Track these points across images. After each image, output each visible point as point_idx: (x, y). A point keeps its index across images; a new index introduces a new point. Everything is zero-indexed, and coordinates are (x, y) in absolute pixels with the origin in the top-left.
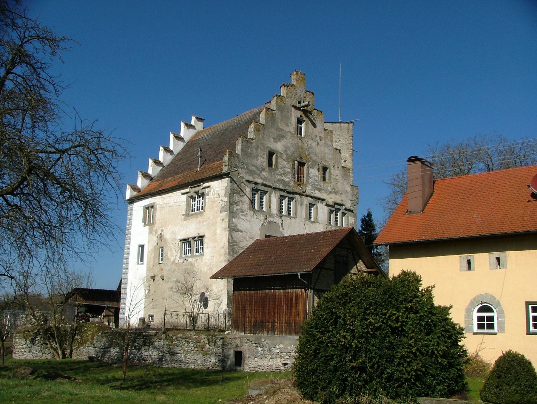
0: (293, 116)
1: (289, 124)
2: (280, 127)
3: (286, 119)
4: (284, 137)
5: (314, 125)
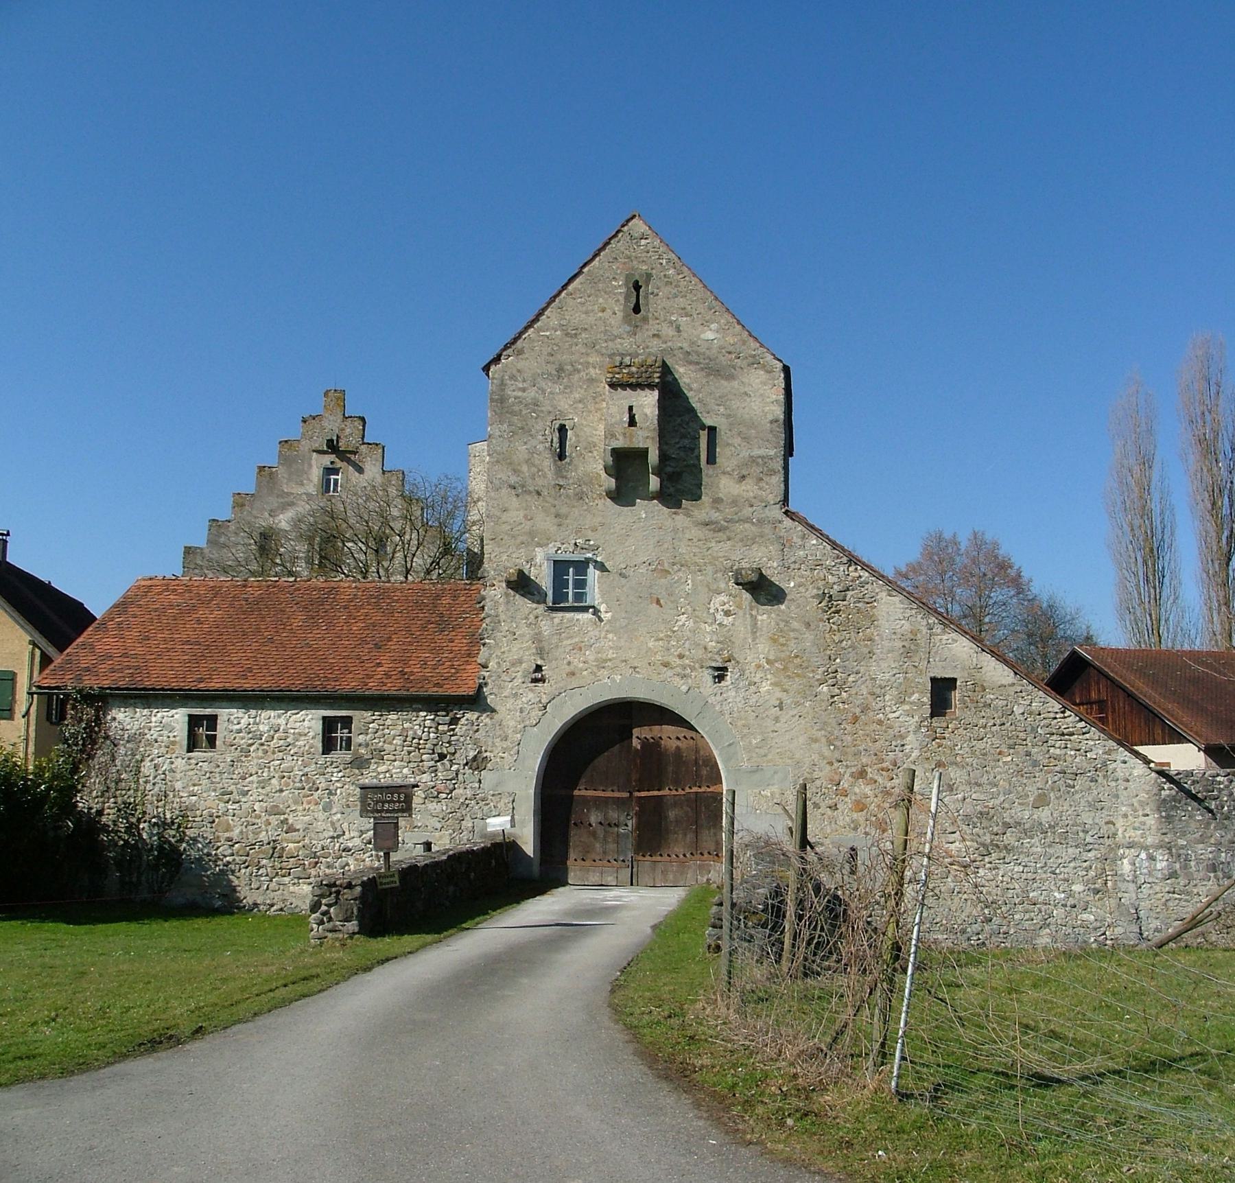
0: (315, 467)
1: (305, 482)
2: (286, 490)
3: (299, 476)
4: (292, 504)
5: (360, 470)
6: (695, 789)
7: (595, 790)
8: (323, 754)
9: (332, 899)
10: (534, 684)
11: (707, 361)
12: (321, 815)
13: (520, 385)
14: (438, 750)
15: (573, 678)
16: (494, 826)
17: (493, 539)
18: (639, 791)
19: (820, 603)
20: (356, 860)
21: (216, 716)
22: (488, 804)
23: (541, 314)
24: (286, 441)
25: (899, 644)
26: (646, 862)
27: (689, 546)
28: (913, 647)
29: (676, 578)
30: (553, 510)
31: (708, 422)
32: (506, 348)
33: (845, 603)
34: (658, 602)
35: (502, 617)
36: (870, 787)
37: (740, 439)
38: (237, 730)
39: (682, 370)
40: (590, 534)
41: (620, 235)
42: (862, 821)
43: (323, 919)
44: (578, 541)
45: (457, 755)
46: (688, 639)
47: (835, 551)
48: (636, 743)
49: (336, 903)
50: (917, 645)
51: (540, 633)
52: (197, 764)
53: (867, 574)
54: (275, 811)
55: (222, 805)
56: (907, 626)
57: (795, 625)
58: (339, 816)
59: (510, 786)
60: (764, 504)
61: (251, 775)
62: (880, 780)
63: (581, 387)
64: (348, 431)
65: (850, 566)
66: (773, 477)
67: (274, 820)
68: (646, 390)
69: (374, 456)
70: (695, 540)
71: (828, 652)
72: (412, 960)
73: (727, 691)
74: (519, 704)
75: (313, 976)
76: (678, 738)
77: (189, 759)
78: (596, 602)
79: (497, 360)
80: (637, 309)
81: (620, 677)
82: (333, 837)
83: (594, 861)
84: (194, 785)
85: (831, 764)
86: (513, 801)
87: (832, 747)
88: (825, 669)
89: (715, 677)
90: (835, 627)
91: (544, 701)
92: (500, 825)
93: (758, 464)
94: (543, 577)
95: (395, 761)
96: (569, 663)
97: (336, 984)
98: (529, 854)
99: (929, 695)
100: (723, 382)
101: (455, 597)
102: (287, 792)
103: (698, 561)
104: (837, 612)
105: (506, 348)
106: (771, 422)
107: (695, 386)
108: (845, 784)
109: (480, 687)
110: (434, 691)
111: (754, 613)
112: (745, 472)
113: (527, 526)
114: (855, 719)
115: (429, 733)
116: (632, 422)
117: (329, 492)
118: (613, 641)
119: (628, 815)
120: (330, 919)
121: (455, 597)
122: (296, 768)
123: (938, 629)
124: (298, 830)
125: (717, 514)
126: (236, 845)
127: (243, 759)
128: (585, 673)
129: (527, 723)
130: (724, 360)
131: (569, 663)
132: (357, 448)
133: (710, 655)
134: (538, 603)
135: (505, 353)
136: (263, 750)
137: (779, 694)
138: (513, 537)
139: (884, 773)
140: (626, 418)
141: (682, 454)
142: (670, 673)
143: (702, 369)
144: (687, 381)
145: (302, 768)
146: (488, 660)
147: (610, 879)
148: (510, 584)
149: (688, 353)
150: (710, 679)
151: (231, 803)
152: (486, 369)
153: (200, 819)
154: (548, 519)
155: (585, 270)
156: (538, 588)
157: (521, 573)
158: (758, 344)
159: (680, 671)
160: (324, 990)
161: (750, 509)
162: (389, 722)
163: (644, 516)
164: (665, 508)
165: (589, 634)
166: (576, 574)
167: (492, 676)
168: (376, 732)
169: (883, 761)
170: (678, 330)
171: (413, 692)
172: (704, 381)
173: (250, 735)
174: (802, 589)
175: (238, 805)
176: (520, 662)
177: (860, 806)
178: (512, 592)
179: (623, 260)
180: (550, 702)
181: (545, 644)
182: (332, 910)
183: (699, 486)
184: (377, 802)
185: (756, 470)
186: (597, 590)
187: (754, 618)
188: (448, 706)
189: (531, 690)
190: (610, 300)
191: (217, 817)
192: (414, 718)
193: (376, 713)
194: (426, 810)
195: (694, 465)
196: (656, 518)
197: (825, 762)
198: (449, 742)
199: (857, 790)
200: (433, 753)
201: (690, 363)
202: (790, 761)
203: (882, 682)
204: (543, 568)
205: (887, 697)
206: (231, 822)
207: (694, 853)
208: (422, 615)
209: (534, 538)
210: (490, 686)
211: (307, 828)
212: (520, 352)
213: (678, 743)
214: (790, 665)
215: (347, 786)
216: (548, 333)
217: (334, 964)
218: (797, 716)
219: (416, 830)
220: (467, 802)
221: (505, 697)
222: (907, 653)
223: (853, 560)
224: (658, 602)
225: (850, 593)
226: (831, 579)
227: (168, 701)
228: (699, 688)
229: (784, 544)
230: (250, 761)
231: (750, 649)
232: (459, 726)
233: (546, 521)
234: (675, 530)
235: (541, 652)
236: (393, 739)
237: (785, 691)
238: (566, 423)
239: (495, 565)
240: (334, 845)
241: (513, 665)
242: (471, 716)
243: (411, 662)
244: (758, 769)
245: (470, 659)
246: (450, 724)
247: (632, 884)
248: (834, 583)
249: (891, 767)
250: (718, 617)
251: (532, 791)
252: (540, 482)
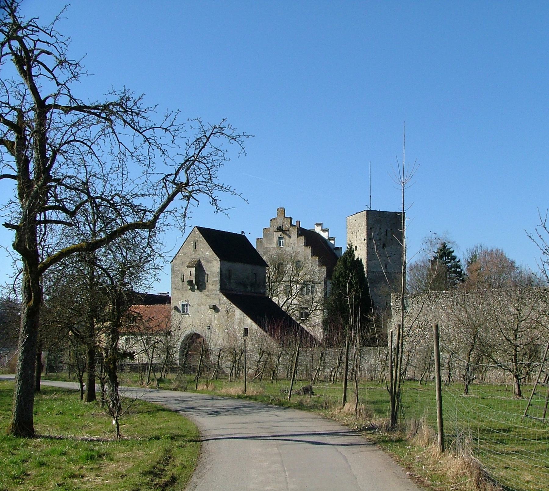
3: (270, 241)
5: (290, 237)
31: (207, 273)
57: (221, 317)
64: (285, 223)
80: (195, 248)
94: (180, 308)
113: (177, 297)
116: (191, 275)
130: (210, 259)
185: (215, 283)
209: (179, 299)
212: (176, 259)
224: (199, 312)
252: (180, 287)
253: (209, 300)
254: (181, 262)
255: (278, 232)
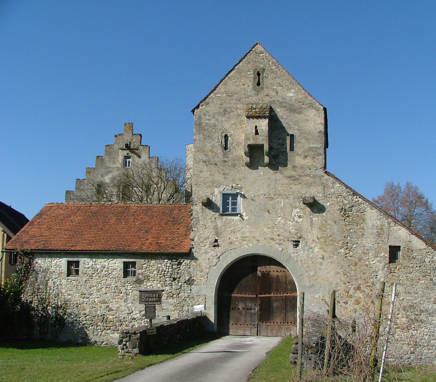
0: (120, 156)
2: (108, 166)
3: (114, 160)
4: (111, 172)
5: (140, 157)
6: (285, 295)
7: (241, 294)
8: (124, 277)
9: (127, 339)
10: (214, 248)
11: (289, 106)
12: (123, 304)
13: (208, 118)
14: (173, 276)
15: (232, 245)
16: (197, 309)
17: (196, 185)
18: (261, 295)
19: (341, 212)
20: (138, 323)
21: (79, 261)
22: (194, 300)
23: (217, 87)
24: (108, 145)
25: (375, 231)
26: (264, 326)
27: (282, 187)
28: (381, 232)
29: (276, 201)
30: (222, 172)
31: (290, 132)
32: (202, 102)
33: (351, 212)
34: (268, 211)
35: (200, 218)
36: (362, 294)
37: (304, 140)
38: (87, 267)
39: (278, 110)
40: (238, 182)
41: (251, 52)
42: (358, 308)
43: (124, 347)
44: (233, 185)
45: (181, 279)
46: (282, 228)
47: (347, 189)
48: (259, 273)
49: (129, 341)
50: (383, 231)
51: (217, 225)
52: (71, 282)
53: (361, 200)
54: (104, 302)
55: (81, 299)
56: (379, 223)
57: (329, 222)
58: (131, 304)
59: (204, 292)
60: (316, 169)
61: (94, 287)
62: (366, 291)
63: (234, 118)
64: (134, 140)
65: (354, 196)
66: (320, 156)
67: (103, 306)
68: (263, 119)
69: (145, 151)
70: (285, 184)
71: (344, 234)
72: (162, 365)
73: (300, 251)
74: (208, 257)
75: (120, 371)
76: (277, 271)
77: (68, 279)
78: (241, 212)
79: (198, 107)
80: (259, 84)
81: (252, 244)
82: (128, 314)
83: (241, 325)
84: (70, 291)
85: (345, 283)
86: (205, 298)
87: (346, 276)
88: (343, 242)
89: (294, 245)
90: (347, 223)
91: (219, 255)
92: (200, 309)
93: (313, 151)
94: (218, 201)
95: (154, 281)
96: (229, 239)
97: (129, 374)
98: (212, 321)
99: (388, 253)
100: (296, 115)
101: (180, 210)
102: (109, 294)
103: (286, 193)
104: (349, 216)
105: (202, 102)
106: (319, 132)
107: (284, 117)
108: (351, 293)
109: (191, 249)
110: (170, 251)
111: (311, 217)
112: (306, 154)
113: (211, 179)
114: (356, 264)
115: (169, 269)
116: (257, 133)
117: (126, 166)
118: (249, 229)
119: (255, 305)
120: (127, 348)
121: (180, 210)
122: (112, 284)
123: (393, 224)
124: (114, 310)
125: (295, 173)
126: (88, 317)
127: (90, 280)
128: (236, 243)
129: (211, 265)
130: (297, 105)
131: (229, 239)
132: (138, 147)
133: (292, 235)
134: (216, 212)
135: (201, 104)
136: (98, 276)
137: (322, 253)
138: (205, 183)
139: (368, 288)
140: (254, 131)
141: (279, 147)
142: (274, 243)
143: (287, 110)
144: (281, 114)
145: (115, 283)
146: (194, 238)
147: (248, 333)
148: (204, 204)
149: (281, 103)
150: (292, 246)
151: (85, 298)
152: (193, 111)
153: (73, 305)
154: (220, 175)
155: (236, 68)
156: (216, 205)
157: (208, 199)
158: (312, 98)
159: (278, 242)
160: (124, 377)
161: (309, 171)
162: (152, 264)
163: (262, 174)
164: (271, 171)
165: (238, 226)
166: (232, 199)
167: (196, 244)
168: (146, 268)
169: (368, 282)
170: (277, 92)
171: (162, 251)
172: (288, 115)
173: (93, 270)
174: (333, 206)
175: (88, 299)
176: (208, 238)
177: (358, 302)
178: (204, 208)
179: (253, 63)
180: (221, 255)
181: (219, 230)
182: (128, 343)
183: (287, 160)
184: (146, 298)
185: (312, 154)
186: (241, 206)
187: (311, 219)
188: (177, 257)
189: (213, 250)
190: (247, 80)
191: (80, 304)
192: (162, 263)
193: (146, 260)
194: (168, 302)
195: (284, 152)
196: (267, 175)
197: (342, 283)
198: (177, 273)
199: (356, 295)
200: (171, 277)
201: (282, 107)
202: (327, 282)
203: (368, 248)
204: (218, 197)
205: (370, 254)
206: (85, 307)
207: (285, 322)
208: (166, 218)
209: (214, 184)
210: (195, 249)
211: (117, 309)
212: (208, 104)
213: (278, 273)
214: (328, 240)
215: (134, 292)
216: (220, 95)
217: (128, 366)
218: (330, 263)
219: (164, 310)
220: (185, 299)
221: (202, 253)
222: (379, 235)
223: (355, 194)
224: (268, 211)
225: (354, 208)
226: (345, 202)
227: (59, 255)
228: (287, 249)
229: (325, 186)
230: (93, 280)
231: (310, 233)
232: (182, 266)
233: (219, 176)
234: (276, 180)
235: (217, 234)
236: (154, 272)
237: (325, 251)
238: (228, 134)
239: (197, 196)
240: (129, 317)
241: (205, 239)
242: (186, 261)
243: (161, 238)
244: (313, 286)
245: (187, 237)
246: (178, 265)
247: (257, 335)
248: (347, 204)
249: (371, 285)
250: (296, 218)
251: (213, 294)
252: (216, 159)
253: (296, 188)
254: (221, 110)
255: (124, 150)
